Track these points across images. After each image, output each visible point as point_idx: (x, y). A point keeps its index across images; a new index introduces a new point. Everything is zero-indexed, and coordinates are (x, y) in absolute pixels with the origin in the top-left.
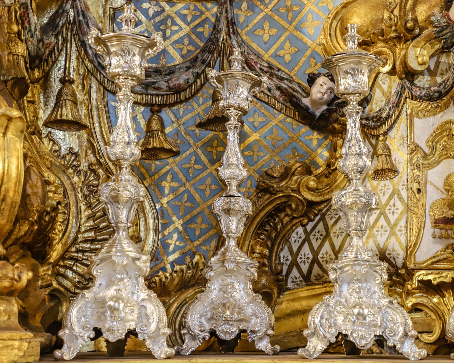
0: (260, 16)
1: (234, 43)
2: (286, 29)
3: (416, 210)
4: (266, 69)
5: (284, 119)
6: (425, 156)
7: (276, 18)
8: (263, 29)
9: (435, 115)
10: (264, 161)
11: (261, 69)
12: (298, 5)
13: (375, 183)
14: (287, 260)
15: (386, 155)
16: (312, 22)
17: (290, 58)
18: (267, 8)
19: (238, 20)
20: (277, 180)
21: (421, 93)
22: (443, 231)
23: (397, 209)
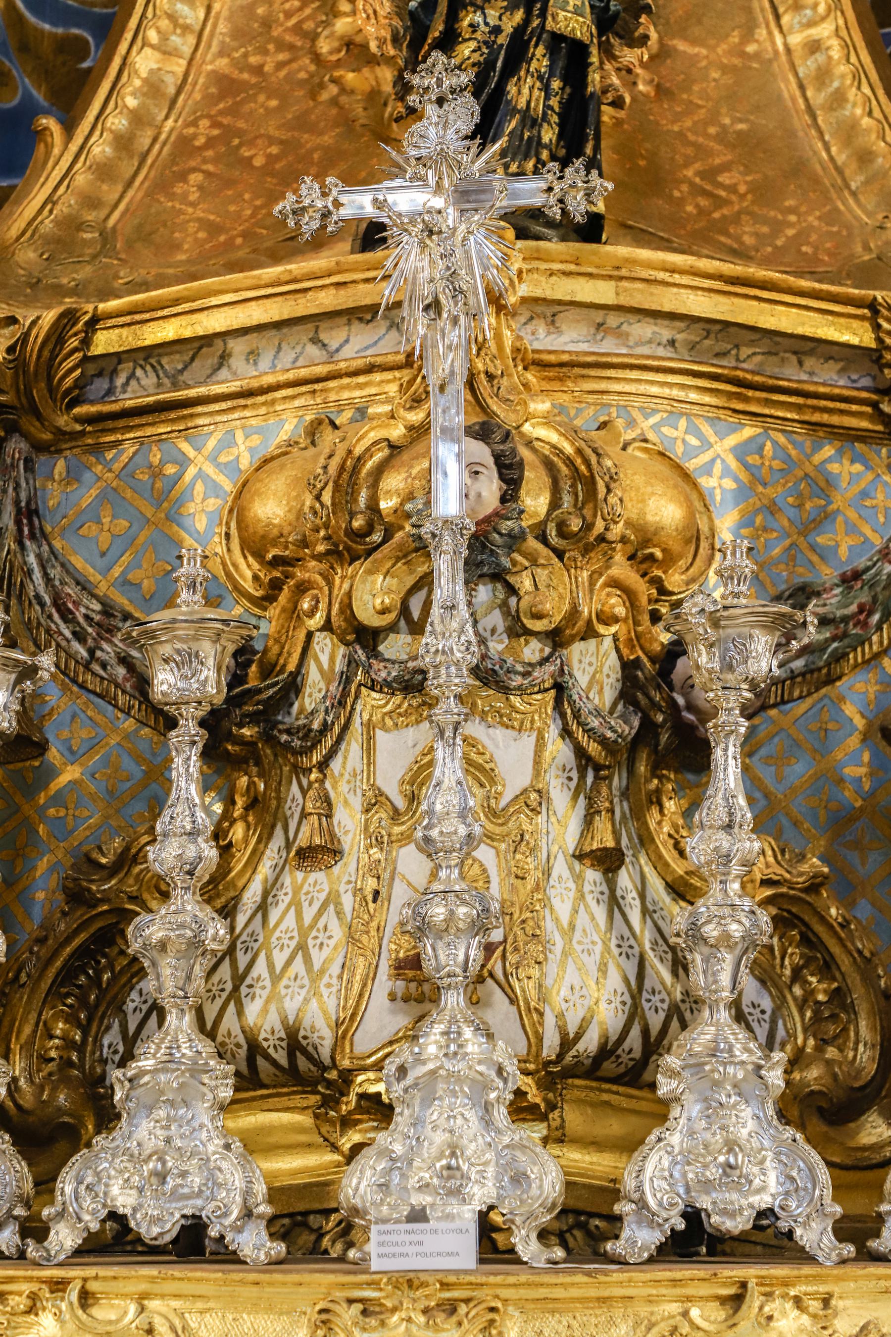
0: (94, 492)
1: (32, 559)
2: (148, 520)
3: (365, 939)
4: (97, 618)
5: (136, 731)
6: (396, 815)
7: (129, 494)
8: (99, 522)
9: (418, 722)
10: (88, 828)
11: (87, 617)
12: (175, 462)
13: (300, 875)
14: (116, 1052)
15: (319, 815)
16: (203, 500)
17: (153, 588)
18: (110, 470)
19: (44, 503)
20: (105, 873)
21: (389, 673)
22: (413, 985)
23: (330, 937)
